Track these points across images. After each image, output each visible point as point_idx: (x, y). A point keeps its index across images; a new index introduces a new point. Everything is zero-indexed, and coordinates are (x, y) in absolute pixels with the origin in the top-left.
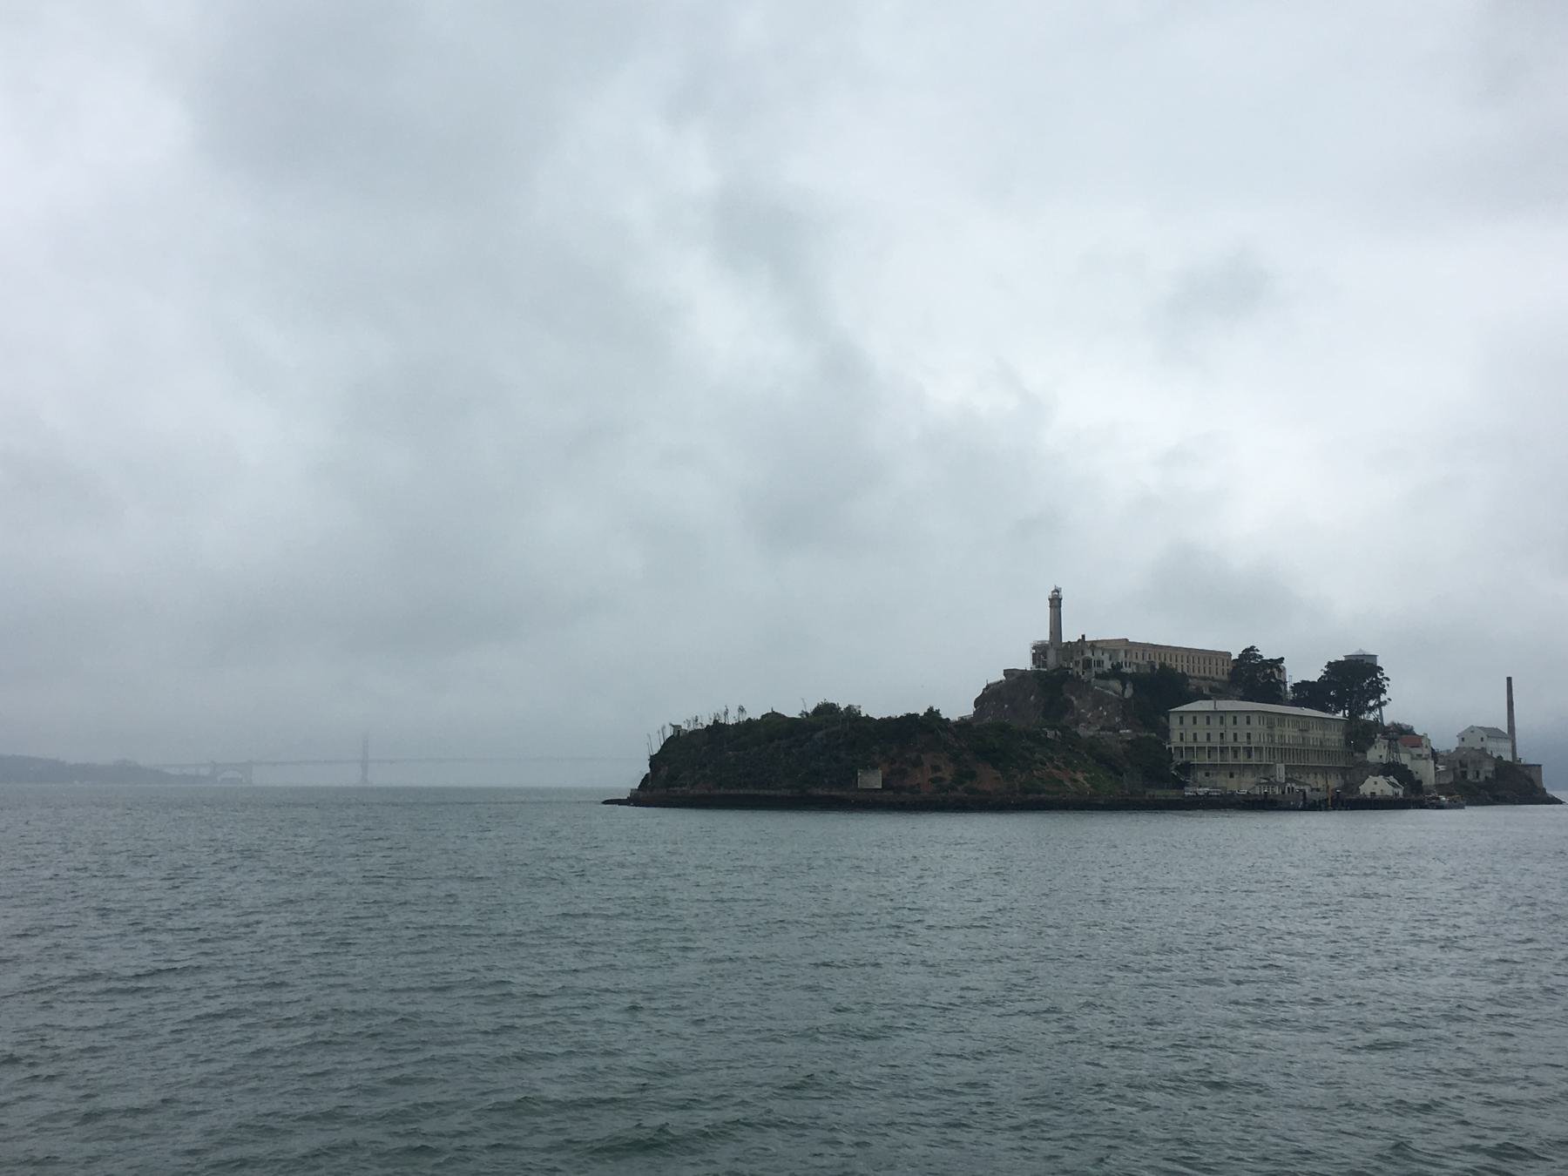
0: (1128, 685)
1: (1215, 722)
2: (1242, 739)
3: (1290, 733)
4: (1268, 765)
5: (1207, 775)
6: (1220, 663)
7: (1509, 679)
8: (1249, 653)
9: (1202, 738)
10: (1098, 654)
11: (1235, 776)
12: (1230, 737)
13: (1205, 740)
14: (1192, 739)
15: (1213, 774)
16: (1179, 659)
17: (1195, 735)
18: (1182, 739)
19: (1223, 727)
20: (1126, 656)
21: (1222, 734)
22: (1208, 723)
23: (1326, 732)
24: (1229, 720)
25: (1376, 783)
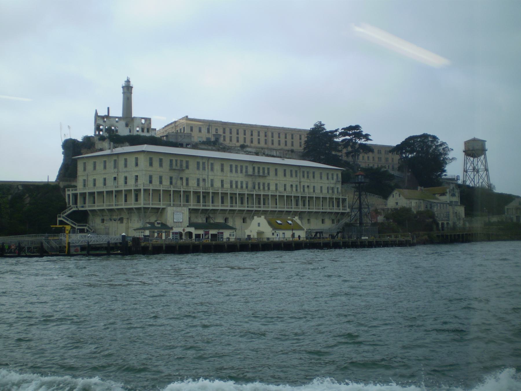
1: (110, 164)
5: (103, 221)
11: (125, 221)
12: (121, 181)
19: (116, 170)
21: (115, 179)
22: (105, 167)
25: (259, 225)
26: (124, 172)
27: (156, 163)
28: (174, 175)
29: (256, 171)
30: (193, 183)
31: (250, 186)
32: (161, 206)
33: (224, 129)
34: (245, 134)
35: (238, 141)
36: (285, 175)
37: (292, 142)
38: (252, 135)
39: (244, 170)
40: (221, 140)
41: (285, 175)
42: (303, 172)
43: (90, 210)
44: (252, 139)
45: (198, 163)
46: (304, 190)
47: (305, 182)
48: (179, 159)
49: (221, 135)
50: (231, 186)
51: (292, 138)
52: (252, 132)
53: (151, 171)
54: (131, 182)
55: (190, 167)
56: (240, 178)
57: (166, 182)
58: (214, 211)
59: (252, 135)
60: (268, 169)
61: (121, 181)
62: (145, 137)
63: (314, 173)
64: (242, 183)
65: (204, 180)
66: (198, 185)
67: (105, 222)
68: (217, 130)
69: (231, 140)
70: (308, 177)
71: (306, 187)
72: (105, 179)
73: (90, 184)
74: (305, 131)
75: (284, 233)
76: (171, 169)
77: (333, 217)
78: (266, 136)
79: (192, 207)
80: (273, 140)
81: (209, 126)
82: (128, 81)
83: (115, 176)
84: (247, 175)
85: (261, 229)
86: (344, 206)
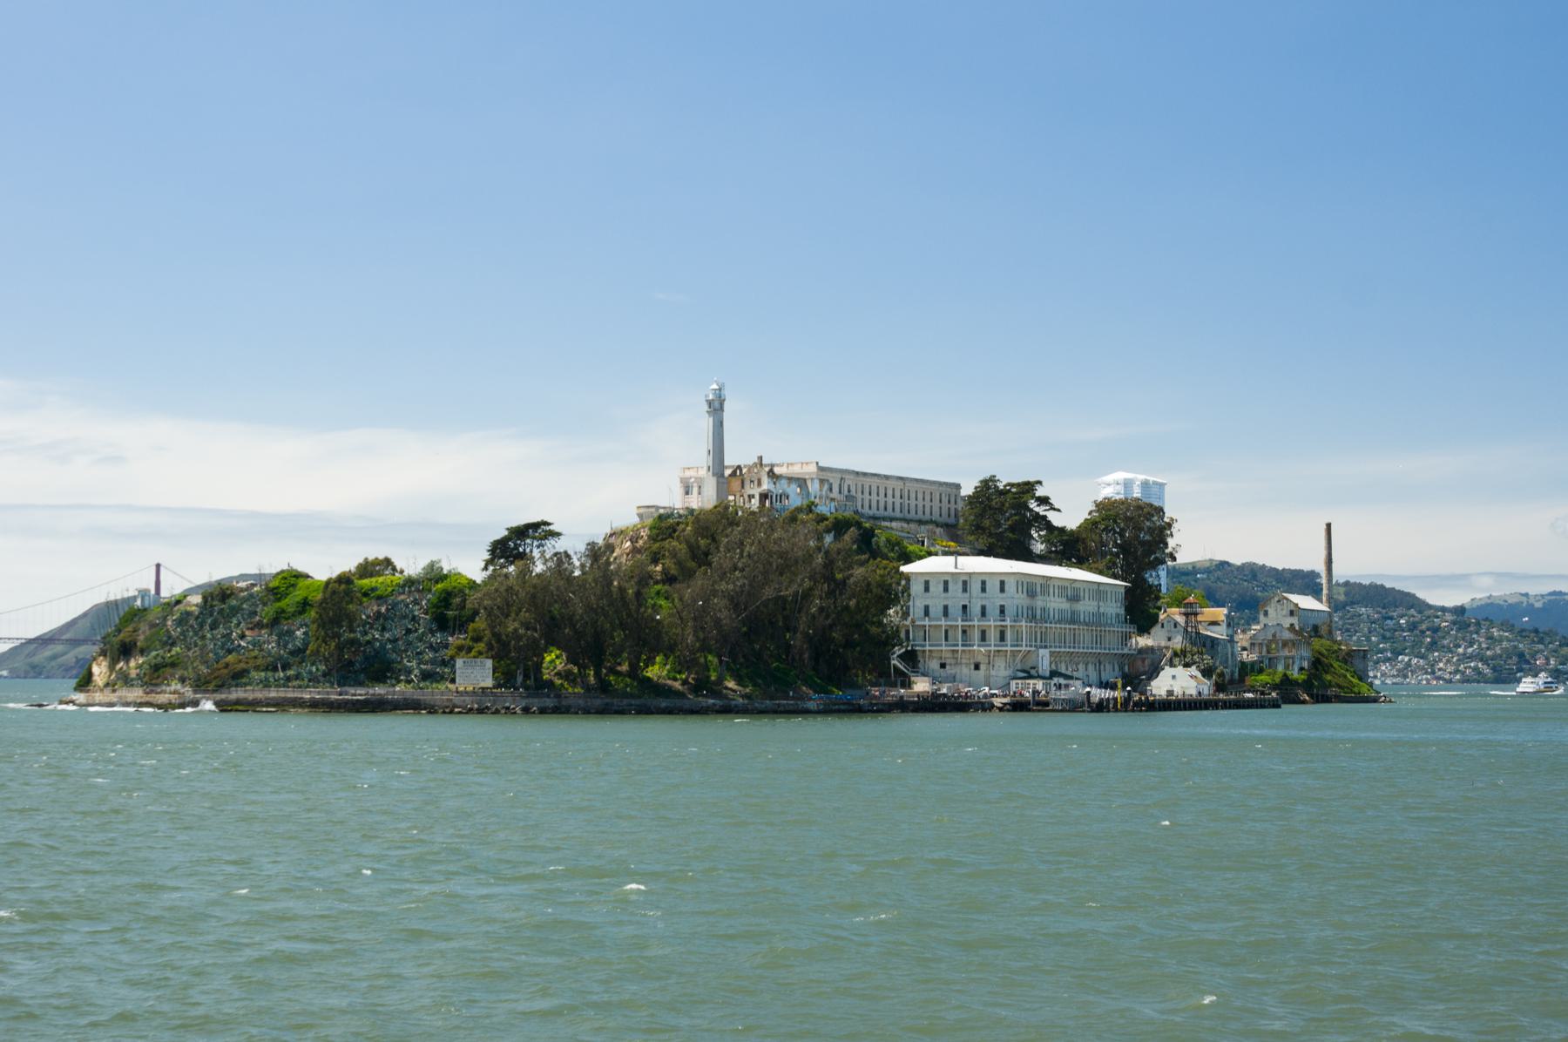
3: (1056, 604)
4: (1029, 651)
5: (943, 666)
6: (945, 500)
7: (1329, 526)
9: (936, 610)
10: (783, 486)
11: (982, 667)
15: (951, 665)
20: (821, 490)
21: (964, 607)
22: (946, 590)
24: (975, 587)
25: (1174, 677)
26: (982, 598)
32: (1033, 649)
37: (931, 507)
43: (930, 651)
44: (886, 502)
51: (931, 500)
61: (976, 610)
67: (947, 667)
72: (946, 608)
78: (901, 497)
80: (909, 504)
81: (842, 479)
83: (964, 603)
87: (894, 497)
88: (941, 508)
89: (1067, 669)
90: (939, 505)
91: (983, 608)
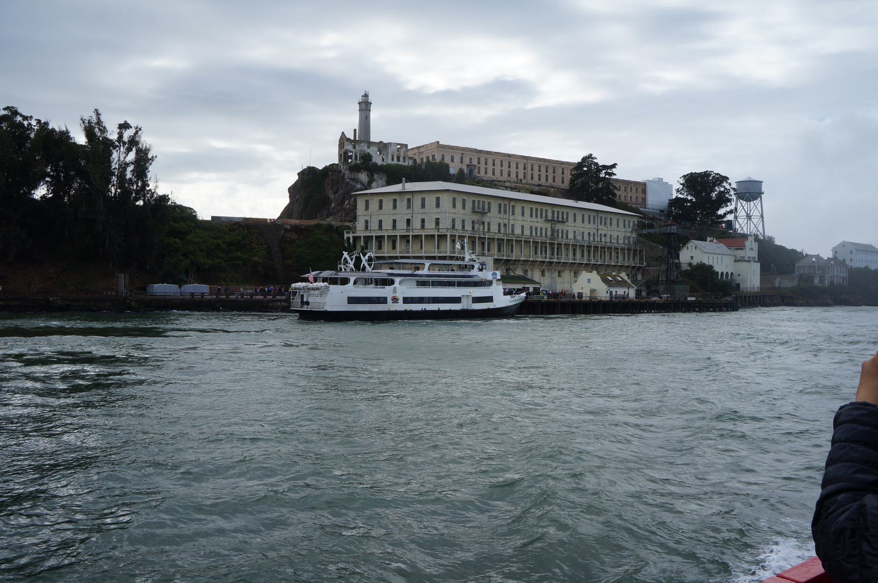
0: (376, 176)
1: (402, 204)
2: (401, 225)
8: (588, 160)
9: (387, 225)
12: (416, 224)
13: (391, 228)
14: (377, 227)
16: (513, 165)
17: (380, 222)
18: (367, 227)
19: (410, 211)
21: (408, 221)
22: (395, 207)
23: (600, 227)
25: (589, 281)
27: (459, 204)
28: (476, 218)
29: (556, 216)
30: (494, 228)
31: (549, 233)
33: (479, 159)
34: (502, 166)
35: (494, 174)
36: (583, 222)
37: (554, 177)
38: (509, 167)
39: (544, 215)
40: (475, 172)
41: (583, 222)
42: (601, 218)
44: (509, 171)
45: (500, 205)
46: (601, 239)
47: (603, 230)
48: (481, 199)
49: (476, 166)
50: (531, 233)
51: (554, 173)
52: (509, 163)
53: (455, 213)
54: (430, 225)
55: (492, 210)
56: (540, 223)
57: (468, 227)
58: (516, 262)
59: (509, 167)
60: (567, 213)
61: (416, 224)
62: (402, 165)
63: (611, 219)
64: (541, 229)
65: (505, 225)
66: (499, 230)
68: (471, 159)
69: (486, 173)
70: (605, 224)
71: (603, 235)
72: (394, 221)
73: (374, 225)
74: (568, 163)
75: (616, 292)
76: (474, 212)
77: (629, 270)
78: (525, 169)
79: (496, 257)
80: (532, 174)
82: (366, 96)
84: (547, 220)
85: (593, 285)
86: (641, 259)
87: (517, 168)
88: (563, 178)
89: (543, 275)
90: (561, 176)
91: (423, 221)
